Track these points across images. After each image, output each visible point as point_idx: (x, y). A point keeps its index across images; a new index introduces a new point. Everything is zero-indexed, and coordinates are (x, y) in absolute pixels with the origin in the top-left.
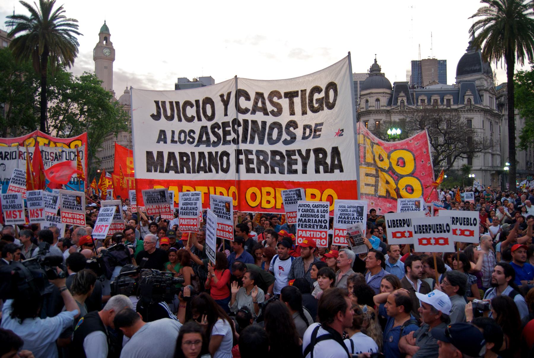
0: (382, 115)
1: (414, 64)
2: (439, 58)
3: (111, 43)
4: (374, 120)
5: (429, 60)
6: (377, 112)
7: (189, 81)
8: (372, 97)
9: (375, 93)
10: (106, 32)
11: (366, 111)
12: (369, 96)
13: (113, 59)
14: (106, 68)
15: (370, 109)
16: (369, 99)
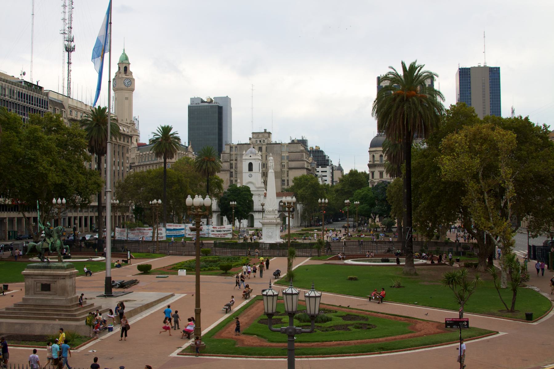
0: (382, 168)
1: (462, 72)
2: (492, 64)
3: (131, 73)
4: (379, 171)
5: (479, 67)
6: (380, 166)
7: (203, 101)
8: (377, 153)
9: (379, 151)
10: (126, 62)
11: (372, 164)
12: (375, 152)
13: (133, 90)
14: (127, 98)
15: (376, 162)
16: (374, 154)
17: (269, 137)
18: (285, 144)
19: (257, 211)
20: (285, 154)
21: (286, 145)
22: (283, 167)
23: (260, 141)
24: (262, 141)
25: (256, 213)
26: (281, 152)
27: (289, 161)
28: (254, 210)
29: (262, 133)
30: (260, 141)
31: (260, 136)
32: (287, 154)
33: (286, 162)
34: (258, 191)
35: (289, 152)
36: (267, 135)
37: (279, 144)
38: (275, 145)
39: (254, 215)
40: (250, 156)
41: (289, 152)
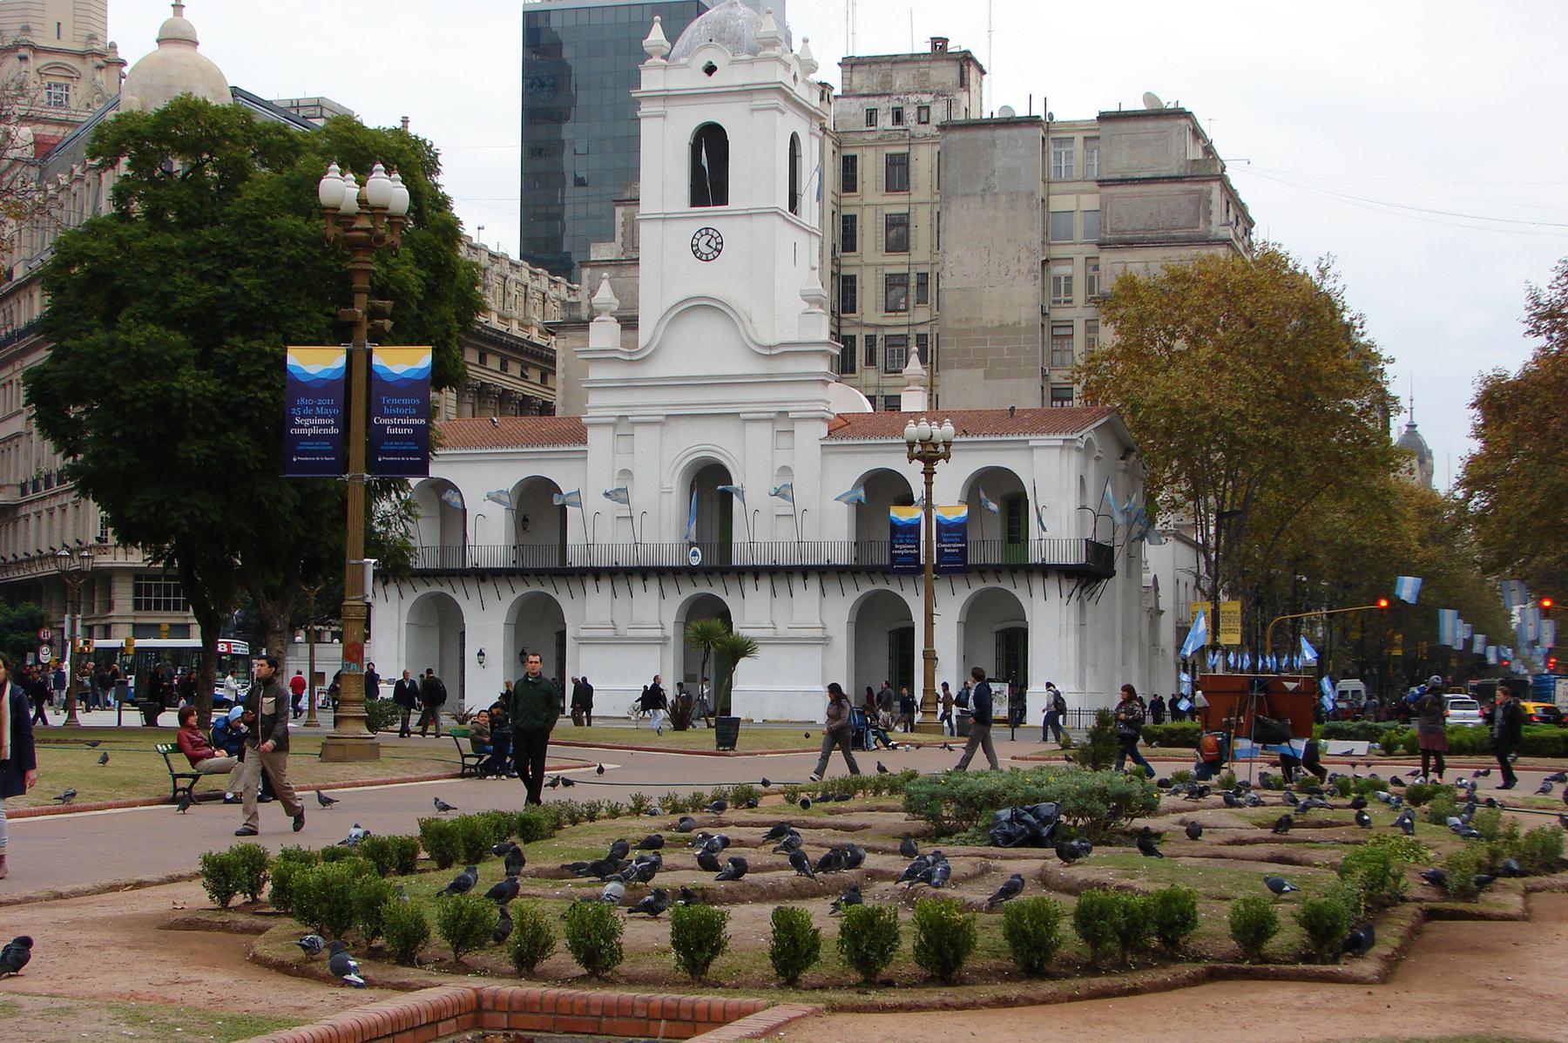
17: (963, 83)
18: (1072, 126)
19: (756, 572)
20: (1079, 202)
21: (1079, 138)
22: (1057, 292)
23: (898, 116)
24: (910, 114)
25: (749, 584)
26: (1046, 182)
27: (1102, 245)
28: (736, 562)
29: (913, 59)
30: (898, 116)
31: (901, 79)
32: (1090, 202)
33: (1080, 261)
34: (769, 381)
35: (1102, 183)
36: (946, 74)
37: (1032, 121)
38: (1002, 133)
39: (732, 602)
40: (710, 70)
41: (1102, 183)
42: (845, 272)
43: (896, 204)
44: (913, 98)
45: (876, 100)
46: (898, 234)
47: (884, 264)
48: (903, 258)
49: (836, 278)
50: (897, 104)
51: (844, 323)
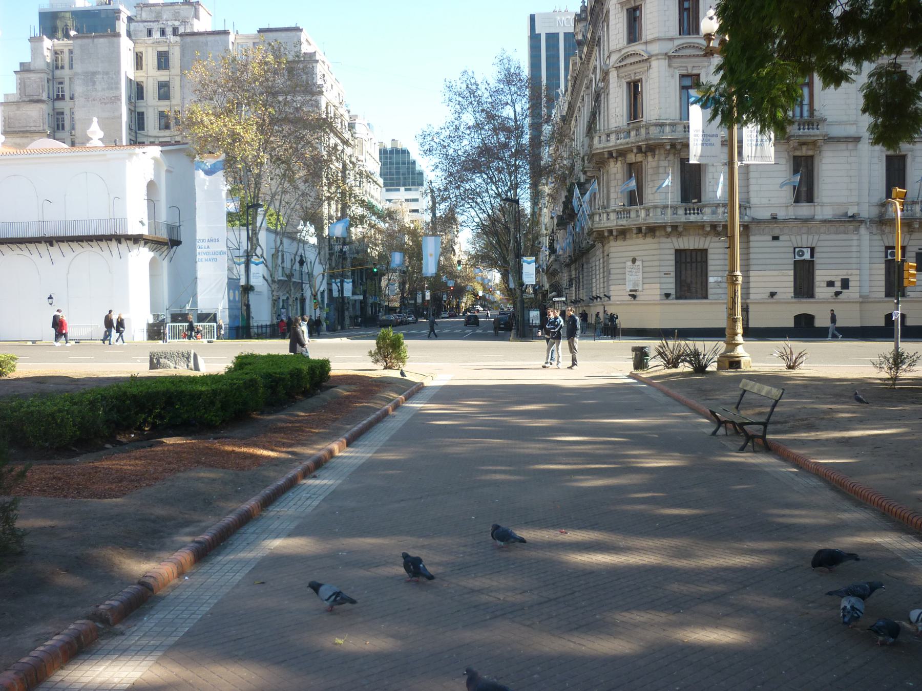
23: (163, 33)
24: (169, 31)
42: (139, 110)
43: (163, 76)
44: (170, 23)
45: (151, 24)
46: (164, 91)
47: (158, 106)
48: (166, 103)
49: (133, 113)
50: (162, 26)
51: (138, 135)
